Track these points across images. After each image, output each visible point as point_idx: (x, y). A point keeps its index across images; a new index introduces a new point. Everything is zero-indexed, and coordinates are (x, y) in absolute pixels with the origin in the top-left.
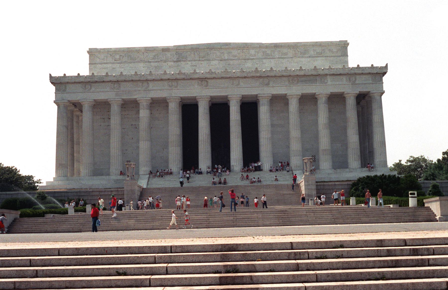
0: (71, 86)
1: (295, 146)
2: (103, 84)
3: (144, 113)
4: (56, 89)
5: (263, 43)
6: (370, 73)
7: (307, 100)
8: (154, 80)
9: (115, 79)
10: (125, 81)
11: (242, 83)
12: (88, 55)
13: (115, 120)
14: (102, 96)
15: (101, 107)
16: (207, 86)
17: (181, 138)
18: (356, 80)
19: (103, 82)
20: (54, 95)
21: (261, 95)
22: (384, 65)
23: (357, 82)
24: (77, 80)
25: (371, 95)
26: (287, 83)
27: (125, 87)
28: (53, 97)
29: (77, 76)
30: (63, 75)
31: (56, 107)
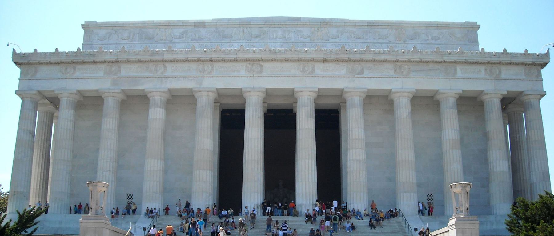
4: (22, 73)
5: (350, 19)
6: (522, 64)
8: (174, 61)
9: (113, 58)
10: (128, 62)
12: (82, 31)
13: (110, 123)
15: (89, 103)
16: (261, 72)
18: (500, 72)
20: (18, 81)
21: (350, 90)
23: (503, 76)
24: (54, 59)
25: (525, 98)
26: (392, 73)
27: (127, 71)
28: (15, 85)
29: (53, 53)
30: (32, 51)
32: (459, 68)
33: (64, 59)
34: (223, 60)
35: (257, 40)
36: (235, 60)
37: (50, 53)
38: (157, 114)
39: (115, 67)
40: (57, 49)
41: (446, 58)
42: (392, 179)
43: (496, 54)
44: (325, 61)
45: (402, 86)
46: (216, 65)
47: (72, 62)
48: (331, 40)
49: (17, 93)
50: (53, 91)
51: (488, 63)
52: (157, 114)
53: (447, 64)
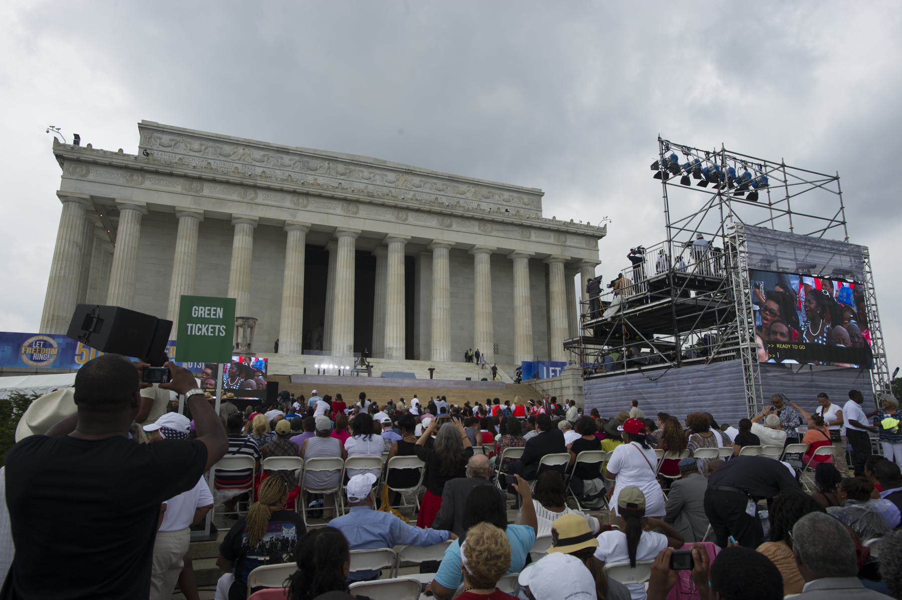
0: (101, 170)
2: (169, 179)
7: (502, 261)
8: (268, 189)
10: (214, 181)
11: (412, 218)
16: (356, 213)
18: (566, 241)
19: (171, 175)
22: (602, 226)
24: (116, 161)
26: (476, 230)
29: (116, 153)
33: (131, 164)
34: (320, 196)
35: (342, 177)
36: (332, 198)
37: (112, 153)
38: (242, 242)
39: (195, 185)
40: (121, 150)
41: (525, 222)
43: (565, 223)
44: (418, 211)
46: (311, 199)
47: (142, 171)
48: (415, 189)
50: (114, 199)
51: (558, 231)
52: (242, 242)
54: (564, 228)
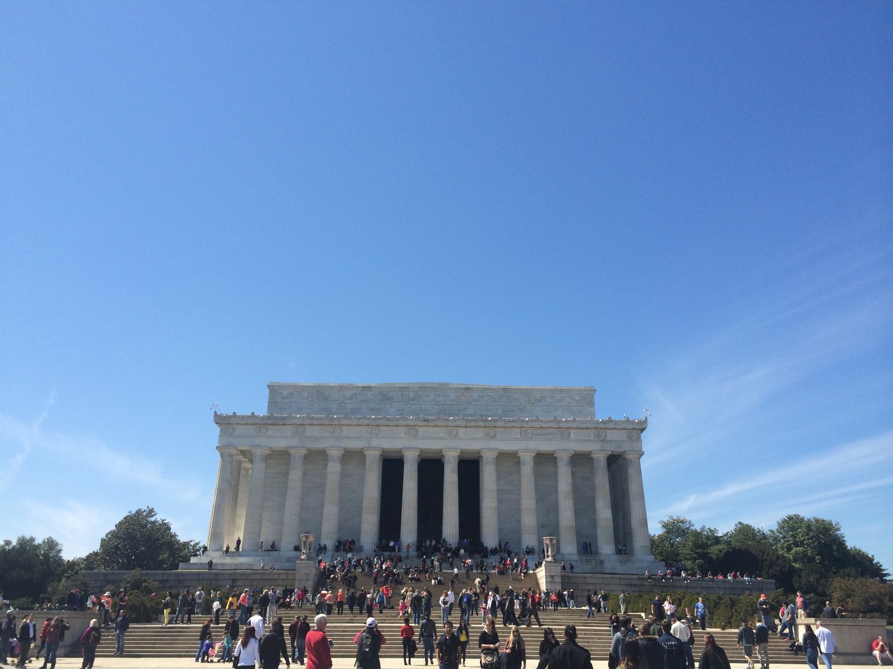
0: (242, 427)
1: (529, 520)
3: (334, 468)
4: (221, 431)
7: (545, 460)
13: (296, 475)
14: (280, 444)
17: (416, 474)
24: (250, 421)
26: (518, 436)
28: (216, 442)
31: (218, 454)
32: (572, 431)
42: (519, 521)
44: (466, 427)
45: (527, 447)
46: (381, 428)
49: (217, 448)
53: (563, 431)
54: (602, 426)
